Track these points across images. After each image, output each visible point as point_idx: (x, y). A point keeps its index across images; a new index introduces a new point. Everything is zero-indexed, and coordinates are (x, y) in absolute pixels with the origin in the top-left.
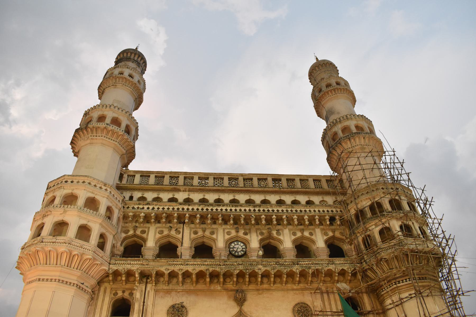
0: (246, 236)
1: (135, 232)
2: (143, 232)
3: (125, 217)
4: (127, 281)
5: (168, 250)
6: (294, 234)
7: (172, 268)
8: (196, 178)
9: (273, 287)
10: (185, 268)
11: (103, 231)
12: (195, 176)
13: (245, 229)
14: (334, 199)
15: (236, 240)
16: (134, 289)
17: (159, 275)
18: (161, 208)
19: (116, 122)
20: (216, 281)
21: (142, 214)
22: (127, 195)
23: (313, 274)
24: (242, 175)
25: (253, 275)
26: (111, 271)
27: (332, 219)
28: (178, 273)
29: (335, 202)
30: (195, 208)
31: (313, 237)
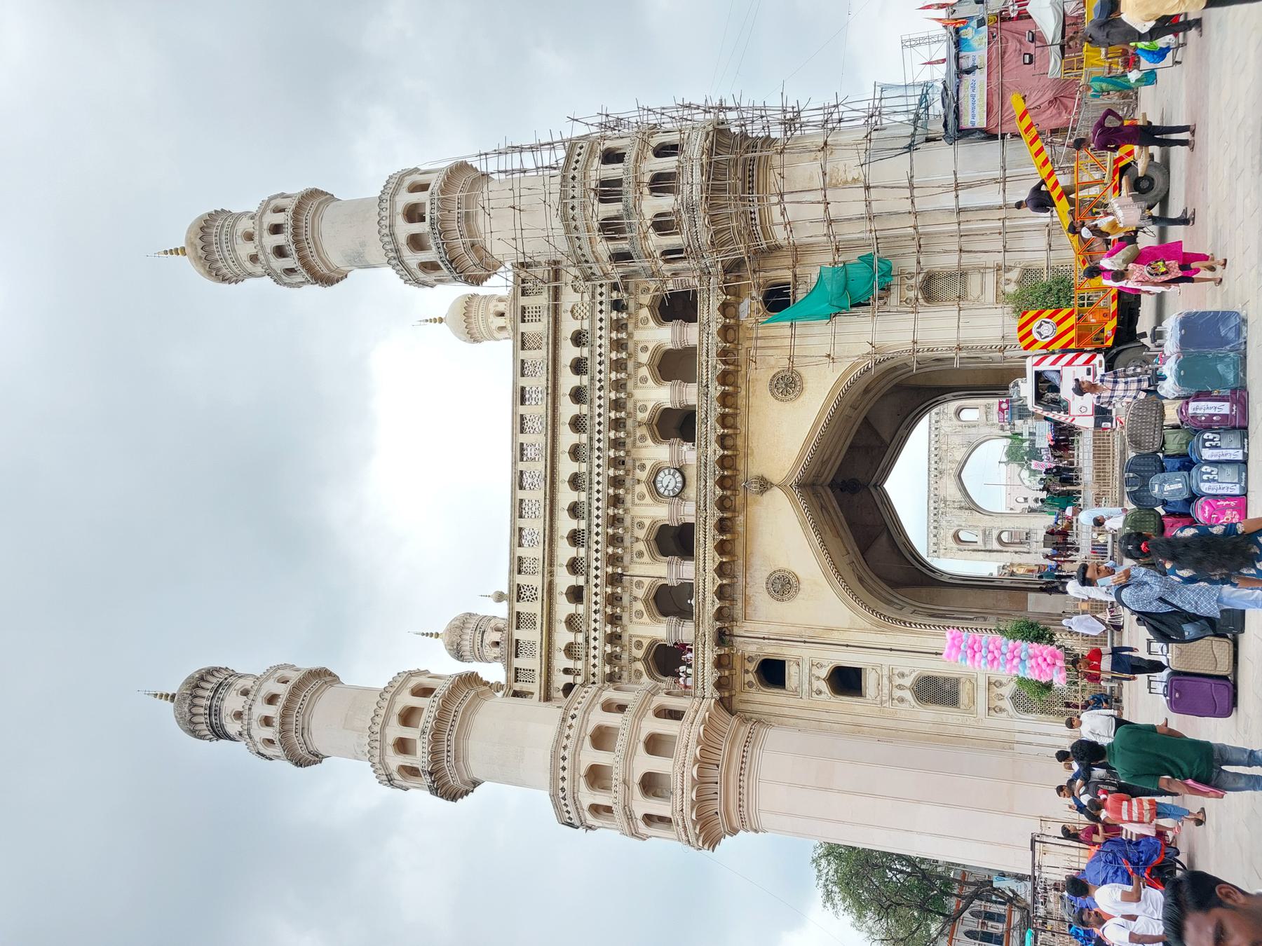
0: (648, 468)
2: (639, 645)
3: (611, 678)
4: (730, 667)
5: (671, 601)
6: (644, 380)
7: (710, 596)
8: (520, 552)
10: (711, 574)
11: (650, 713)
12: (518, 554)
15: (653, 483)
16: (743, 655)
17: (720, 615)
18: (594, 616)
19: (408, 717)
20: (729, 523)
21: (608, 649)
22: (560, 680)
23: (725, 362)
24: (514, 463)
25: (723, 462)
26: (717, 695)
27: (617, 306)
28: (721, 586)
30: (595, 555)
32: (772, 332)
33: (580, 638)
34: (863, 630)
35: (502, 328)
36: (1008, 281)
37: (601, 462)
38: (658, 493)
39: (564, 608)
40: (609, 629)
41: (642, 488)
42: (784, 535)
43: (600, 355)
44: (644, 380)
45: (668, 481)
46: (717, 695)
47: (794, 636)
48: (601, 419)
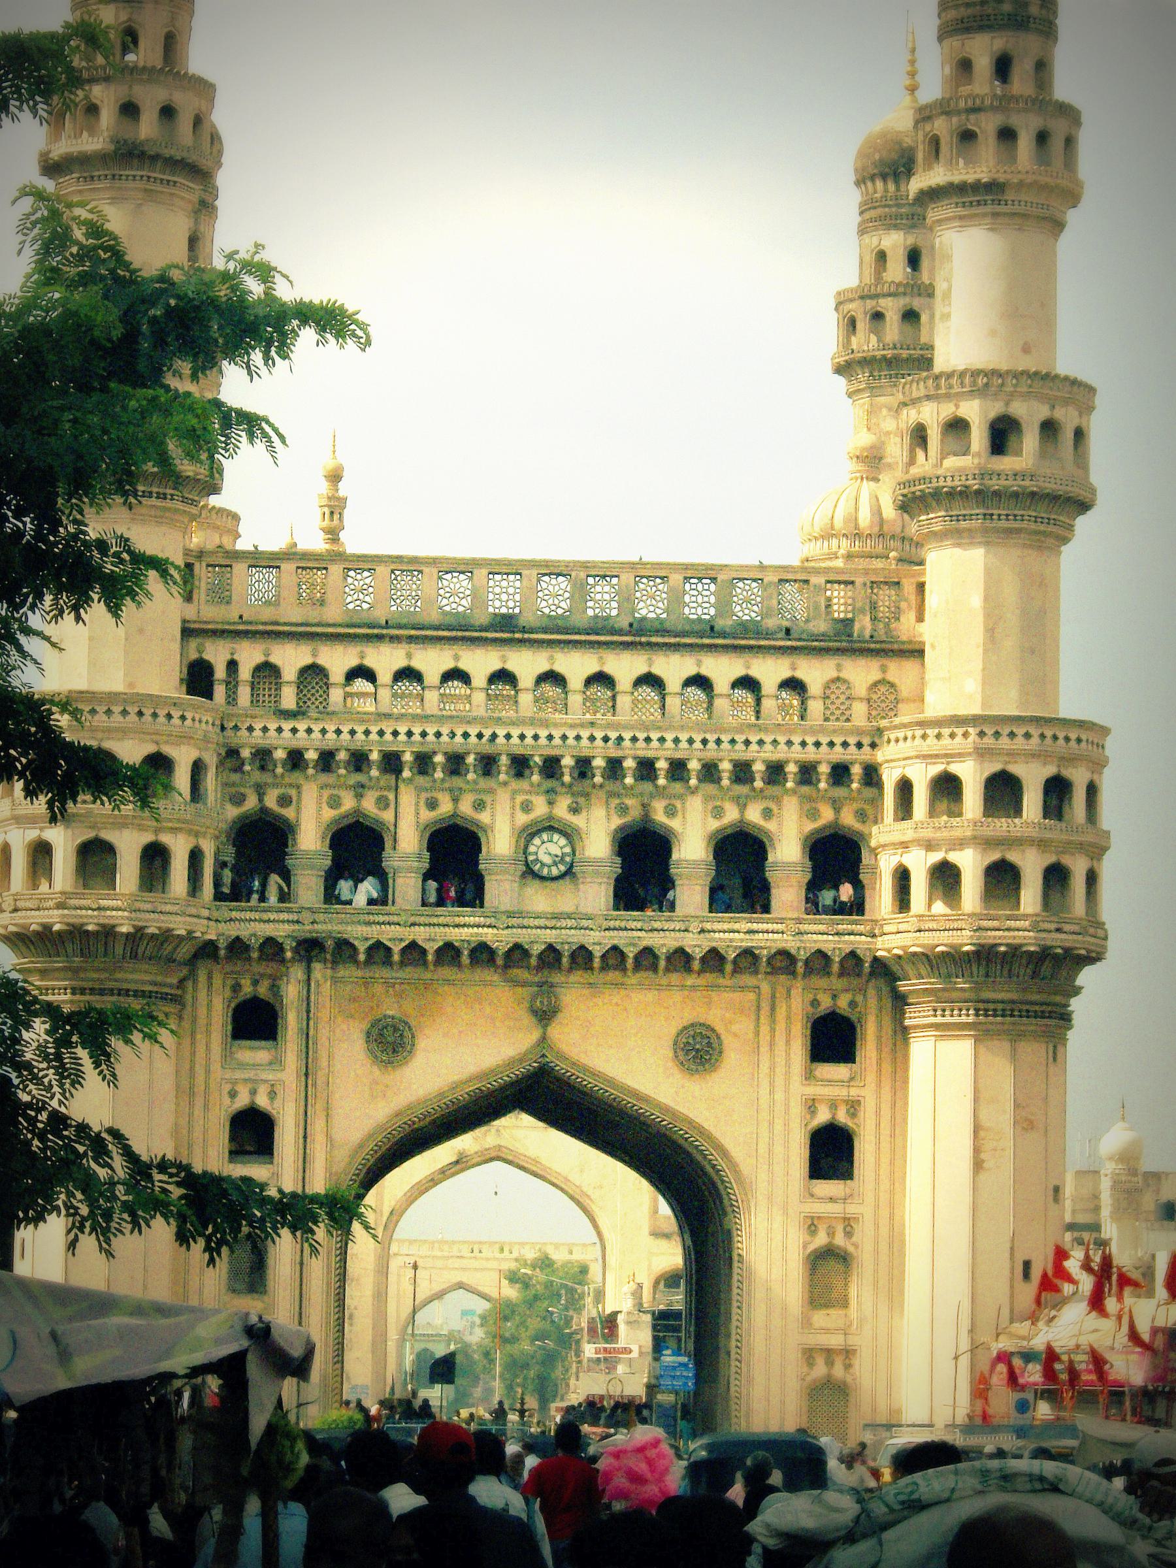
1: (261, 800)
2: (285, 801)
6: (718, 812)
9: (633, 979)
12: (426, 570)
13: (573, 794)
14: (875, 675)
15: (550, 826)
17: (344, 949)
18: (331, 728)
21: (280, 754)
24: (585, 565)
27: (840, 773)
29: (876, 684)
30: (431, 731)
31: (771, 826)
32: (781, 1026)
33: (289, 699)
34: (329, 1160)
35: (882, 256)
36: (830, 1363)
37: (585, 742)
38: (532, 835)
39: (338, 660)
40: (311, 755)
41: (540, 808)
42: (466, 1042)
43: (761, 742)
44: (718, 812)
45: (548, 849)
46: (222, 944)
47: (316, 1059)
48: (655, 744)
